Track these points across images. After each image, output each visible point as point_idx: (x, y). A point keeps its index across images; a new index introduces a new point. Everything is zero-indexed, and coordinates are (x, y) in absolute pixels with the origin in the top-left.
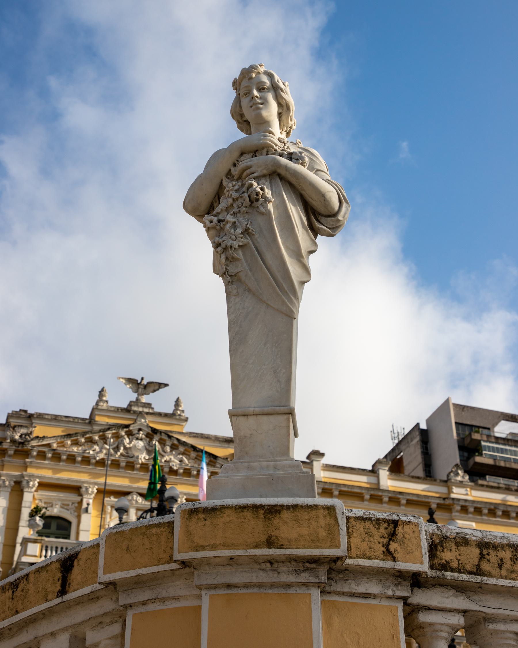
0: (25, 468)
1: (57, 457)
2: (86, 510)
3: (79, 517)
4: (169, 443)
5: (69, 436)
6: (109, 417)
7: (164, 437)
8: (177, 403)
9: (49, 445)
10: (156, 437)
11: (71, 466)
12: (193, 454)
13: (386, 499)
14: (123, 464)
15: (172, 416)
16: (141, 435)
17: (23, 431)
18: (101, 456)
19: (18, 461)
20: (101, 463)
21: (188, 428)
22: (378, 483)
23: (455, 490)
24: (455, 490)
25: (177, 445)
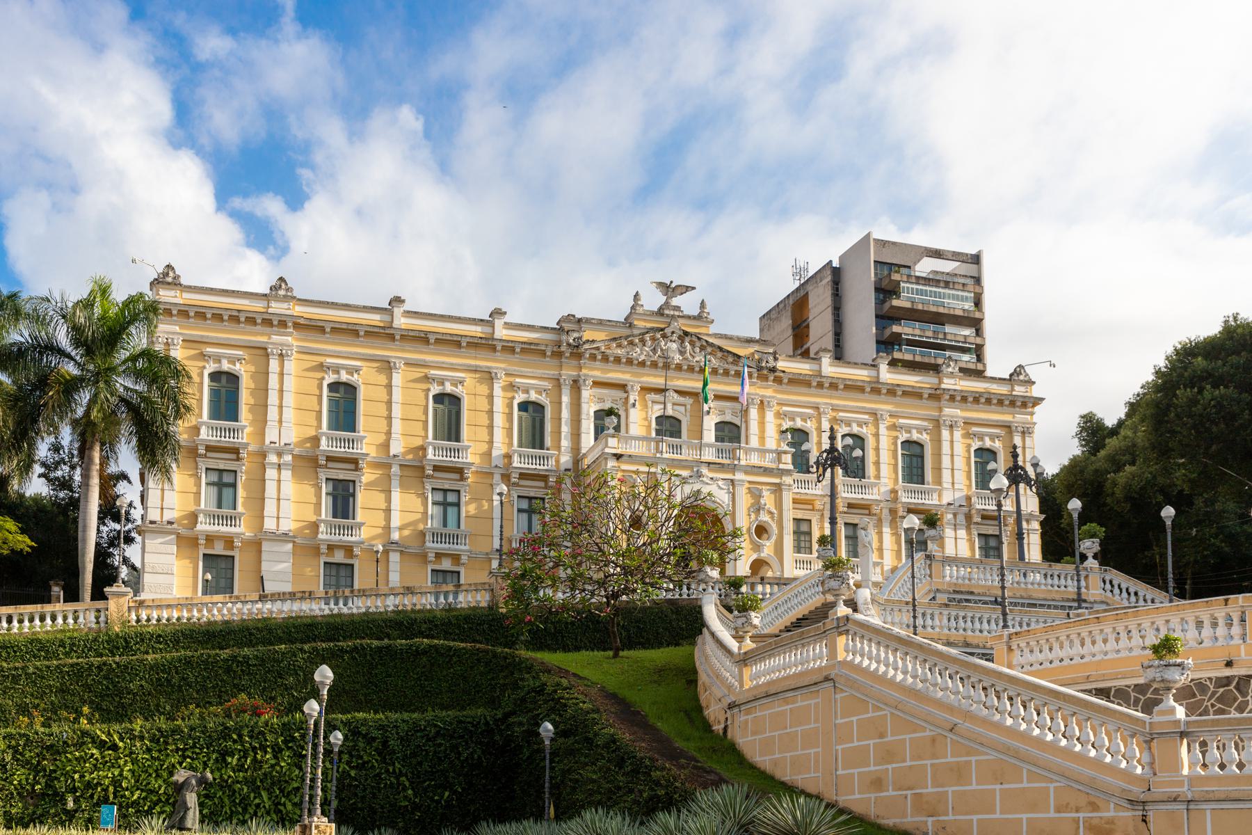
0: (580, 369)
1: (605, 359)
2: (634, 405)
3: (627, 411)
4: (698, 344)
5: (614, 339)
6: (645, 320)
7: (694, 339)
8: (703, 305)
9: (598, 348)
10: (687, 339)
11: (617, 367)
12: (719, 354)
13: (884, 391)
14: (661, 365)
15: (699, 318)
16: (675, 337)
17: (576, 335)
18: (642, 358)
19: (574, 362)
20: (643, 364)
21: (713, 329)
22: (878, 377)
23: (945, 380)
24: (945, 380)
25: (706, 346)
